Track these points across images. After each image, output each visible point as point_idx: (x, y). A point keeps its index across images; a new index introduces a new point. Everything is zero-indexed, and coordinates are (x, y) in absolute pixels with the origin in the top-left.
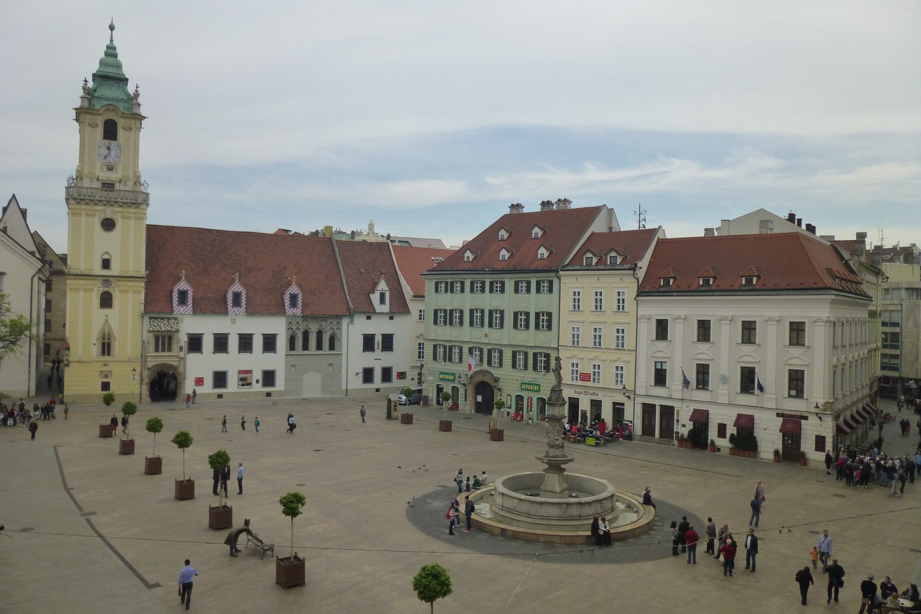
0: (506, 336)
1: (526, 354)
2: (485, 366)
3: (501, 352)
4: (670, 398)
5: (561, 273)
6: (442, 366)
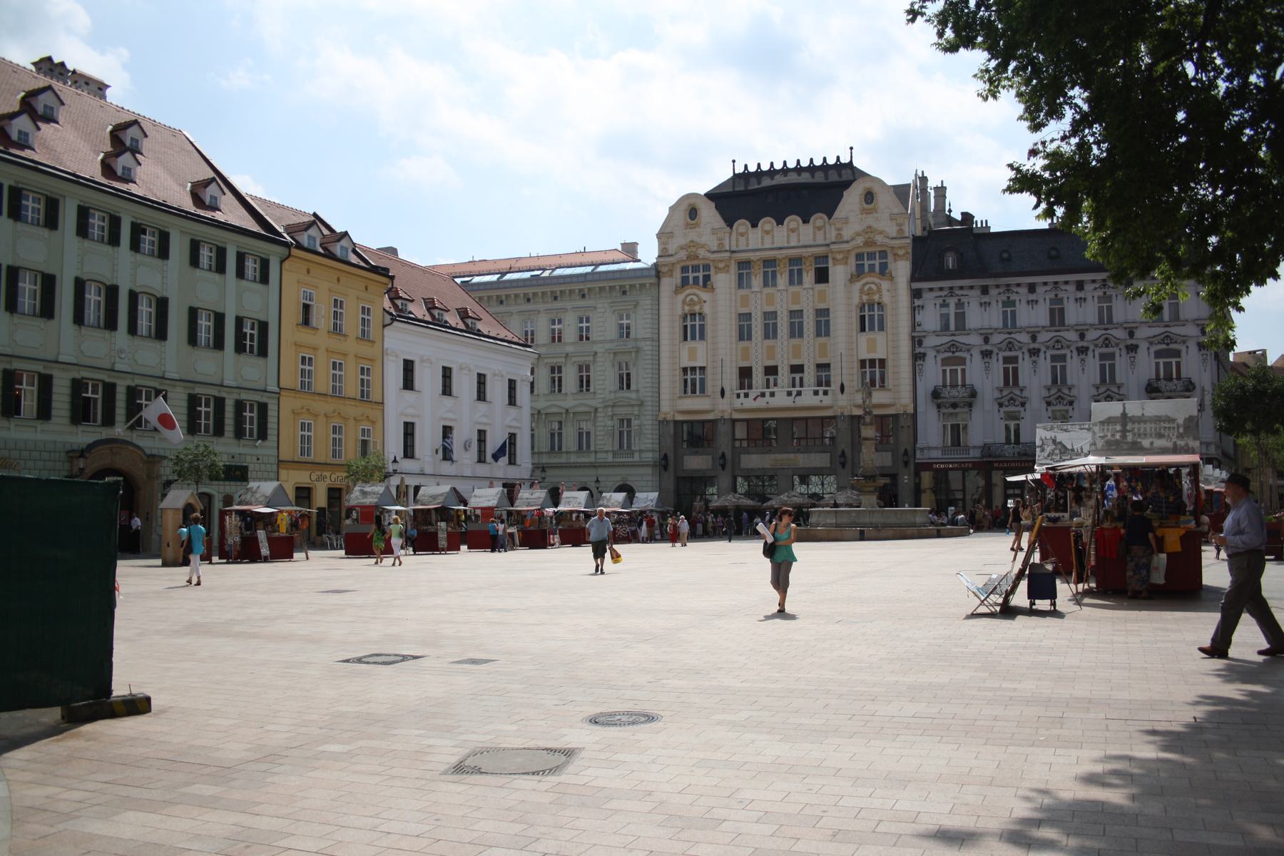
1: (220, 402)
2: (119, 430)
5: (295, 252)
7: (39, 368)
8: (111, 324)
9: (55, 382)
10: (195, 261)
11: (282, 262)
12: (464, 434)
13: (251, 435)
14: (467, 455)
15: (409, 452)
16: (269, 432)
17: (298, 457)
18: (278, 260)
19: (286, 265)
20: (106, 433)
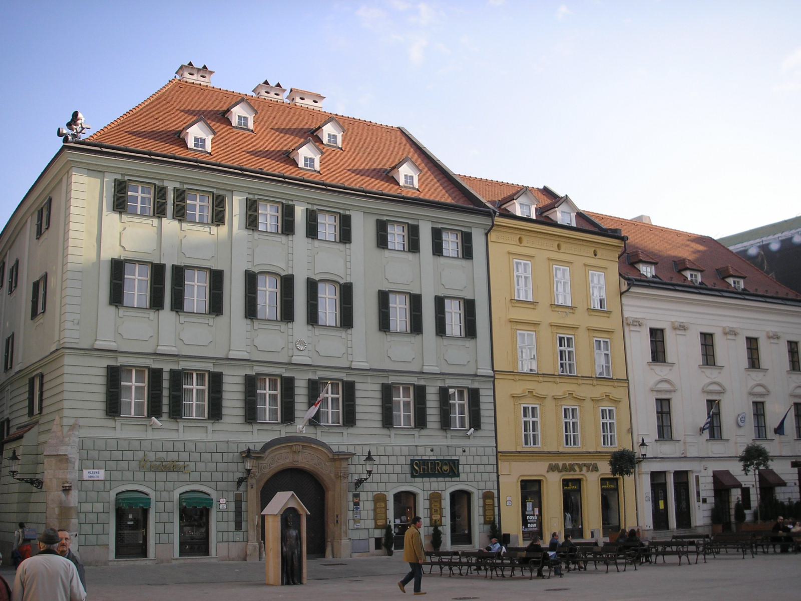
0: (360, 349)
1: (420, 393)
2: (300, 427)
3: (349, 390)
4: (684, 458)
5: (498, 220)
6: (138, 432)
7: (209, 366)
8: (287, 314)
9: (225, 379)
10: (382, 242)
11: (487, 235)
12: (736, 406)
13: (462, 425)
14: (741, 432)
15: (664, 431)
16: (483, 420)
17: (522, 447)
18: (483, 232)
19: (493, 236)
20: (285, 431)
